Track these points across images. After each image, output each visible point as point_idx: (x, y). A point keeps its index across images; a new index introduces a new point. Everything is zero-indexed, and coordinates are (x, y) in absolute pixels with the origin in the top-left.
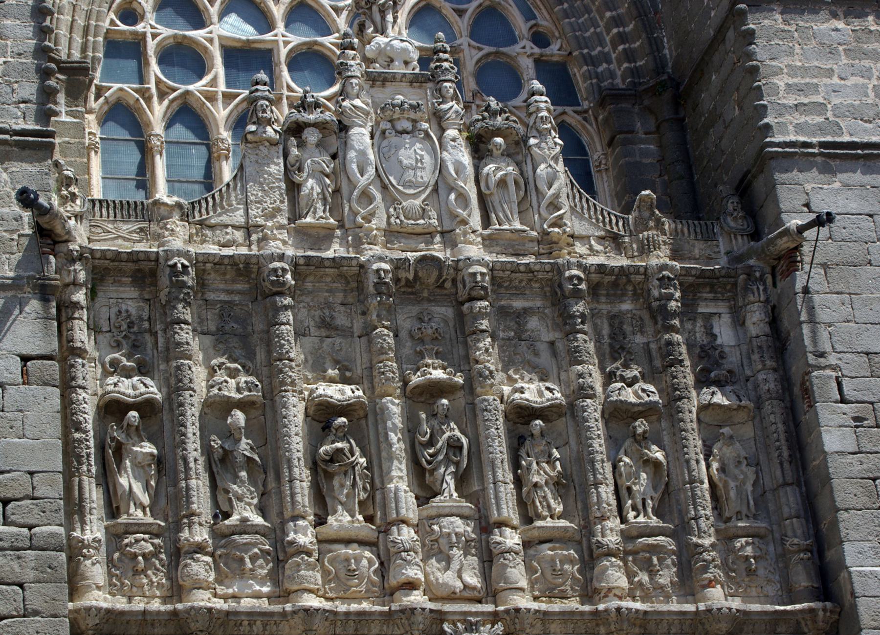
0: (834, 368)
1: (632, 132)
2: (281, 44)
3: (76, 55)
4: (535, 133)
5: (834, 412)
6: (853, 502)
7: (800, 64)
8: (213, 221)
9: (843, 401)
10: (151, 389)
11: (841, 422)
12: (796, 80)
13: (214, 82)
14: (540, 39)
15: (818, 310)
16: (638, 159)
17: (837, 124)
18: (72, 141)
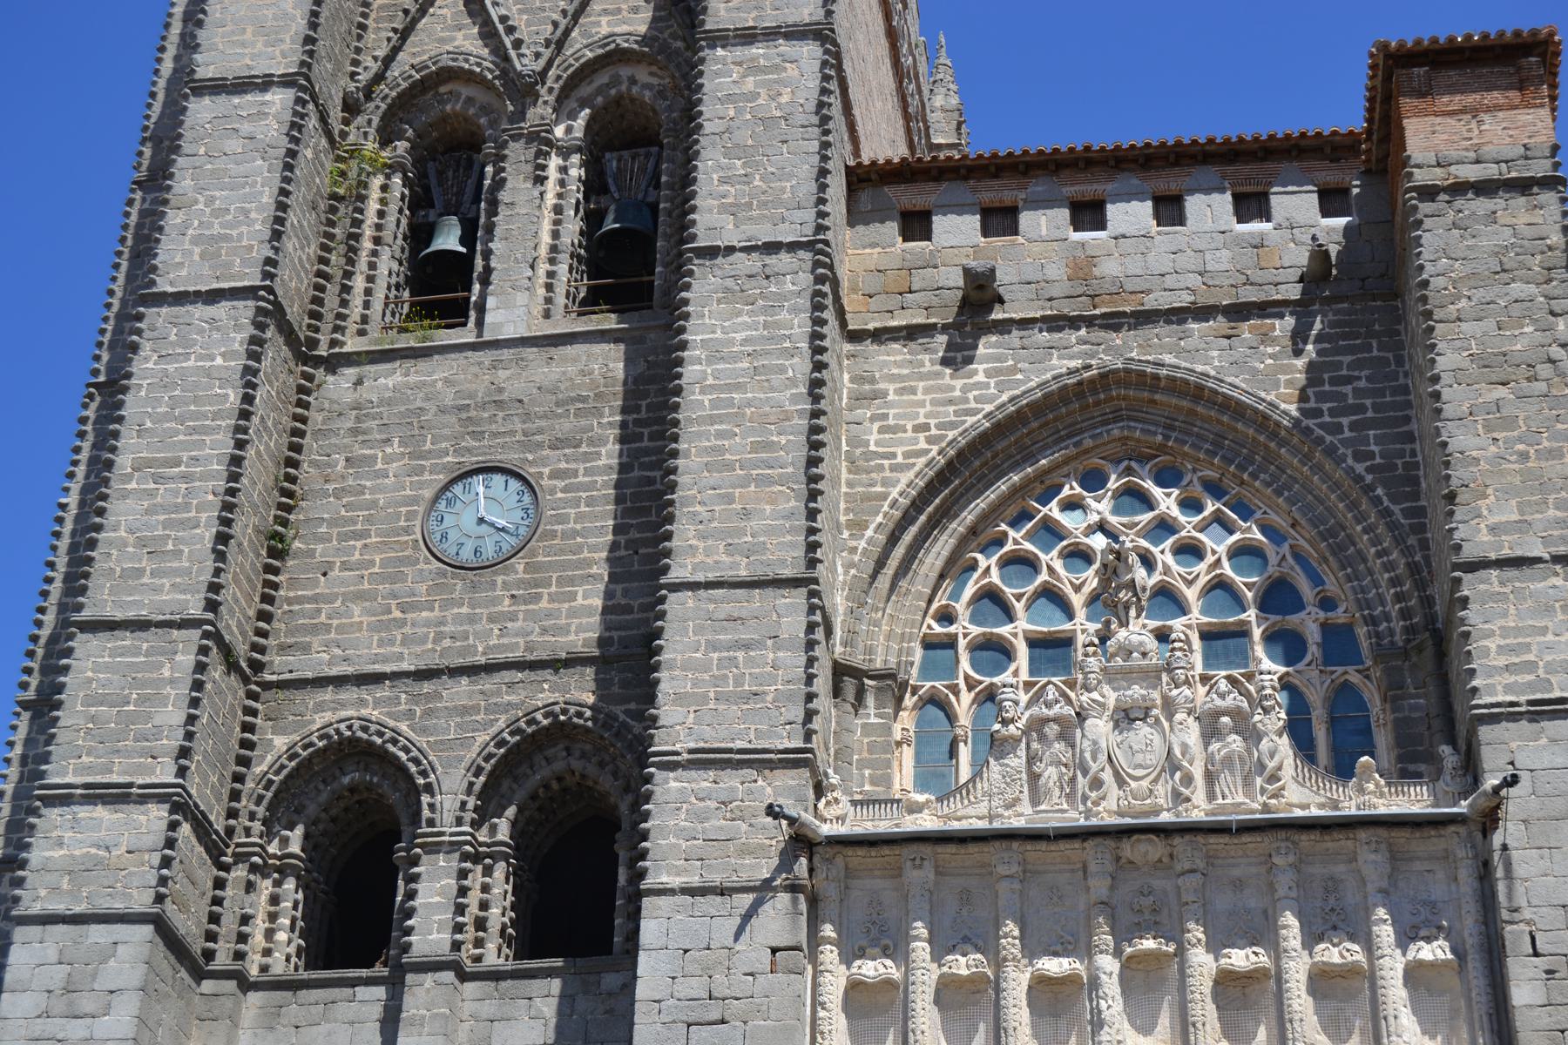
0: (1528, 923)
1: (1401, 688)
2: (1079, 632)
3: (893, 661)
4: (1260, 711)
5: (1525, 966)
7: (1513, 624)
8: (959, 814)
9: (1536, 954)
10: (890, 970)
11: (1531, 973)
12: (1508, 641)
13: (1016, 673)
14: (1327, 603)
15: (1515, 866)
16: (1407, 713)
17: (1548, 681)
18: (878, 739)
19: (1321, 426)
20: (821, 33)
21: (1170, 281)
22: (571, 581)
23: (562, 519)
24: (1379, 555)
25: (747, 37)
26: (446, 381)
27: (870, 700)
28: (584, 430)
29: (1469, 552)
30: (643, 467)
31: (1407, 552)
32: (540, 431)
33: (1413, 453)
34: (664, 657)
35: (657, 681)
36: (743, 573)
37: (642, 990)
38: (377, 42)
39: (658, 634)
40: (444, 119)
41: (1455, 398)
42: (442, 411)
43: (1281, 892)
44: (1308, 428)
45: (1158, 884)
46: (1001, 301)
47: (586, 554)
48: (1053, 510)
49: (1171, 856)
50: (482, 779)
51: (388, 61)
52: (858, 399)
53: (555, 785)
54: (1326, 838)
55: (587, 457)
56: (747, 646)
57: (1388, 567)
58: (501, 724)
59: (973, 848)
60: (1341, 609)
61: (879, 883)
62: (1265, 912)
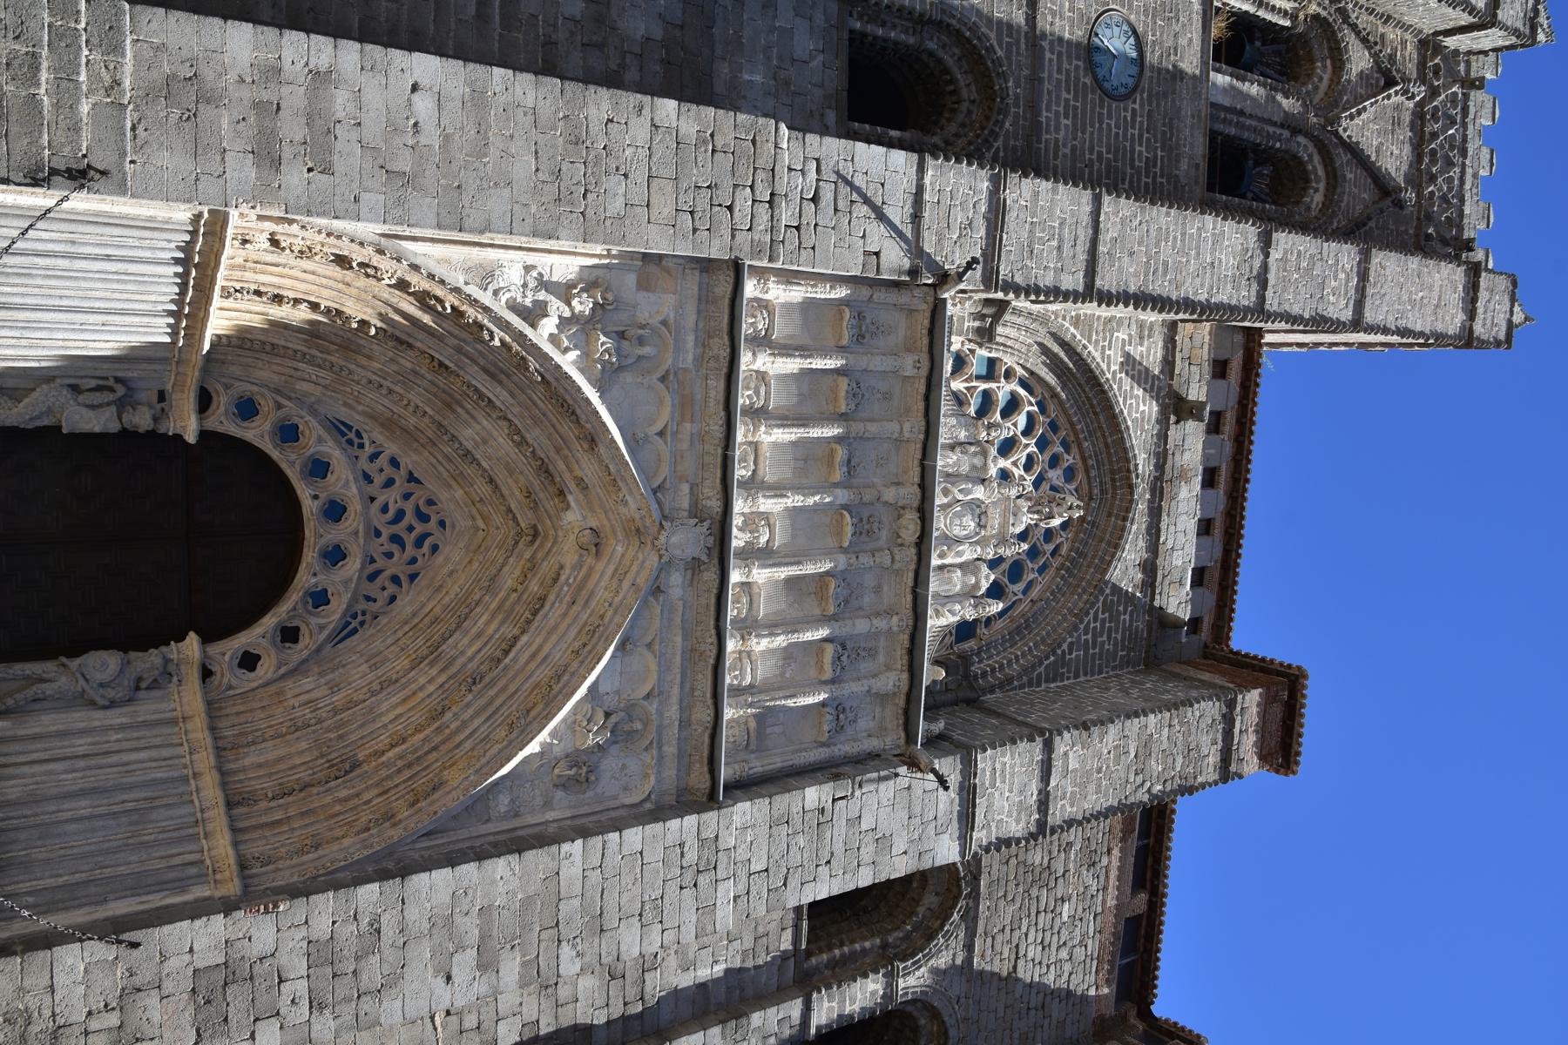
0: (853, 794)
6: (776, 806)
9: (834, 800)
11: (823, 799)
19: (1089, 622)
20: (1357, 324)
21: (1172, 528)
22: (1075, 116)
23: (1110, 117)
24: (1017, 657)
25: (1363, 276)
26: (1191, 40)
27: (977, 324)
28: (1155, 136)
29: (1061, 745)
30: (1132, 175)
31: (1020, 677)
32: (1158, 105)
33: (1068, 678)
34: (1061, 186)
35: (1048, 180)
36: (1102, 249)
37: (861, 147)
38: (1363, 20)
39: (1075, 185)
40: (1312, 61)
41: (1134, 725)
42: (1176, 36)
43: (875, 622)
44: (1087, 614)
45: (884, 534)
46: (1177, 422)
47: (1089, 129)
48: (1059, 449)
49: (902, 545)
50: (968, 34)
51: (1354, 27)
52: (1141, 326)
53: (952, 88)
54: (904, 652)
55: (1141, 136)
56: (1059, 248)
57: (1010, 662)
58: (1000, 53)
59: (921, 405)
60: (984, 631)
61: (902, 332)
62: (860, 608)
